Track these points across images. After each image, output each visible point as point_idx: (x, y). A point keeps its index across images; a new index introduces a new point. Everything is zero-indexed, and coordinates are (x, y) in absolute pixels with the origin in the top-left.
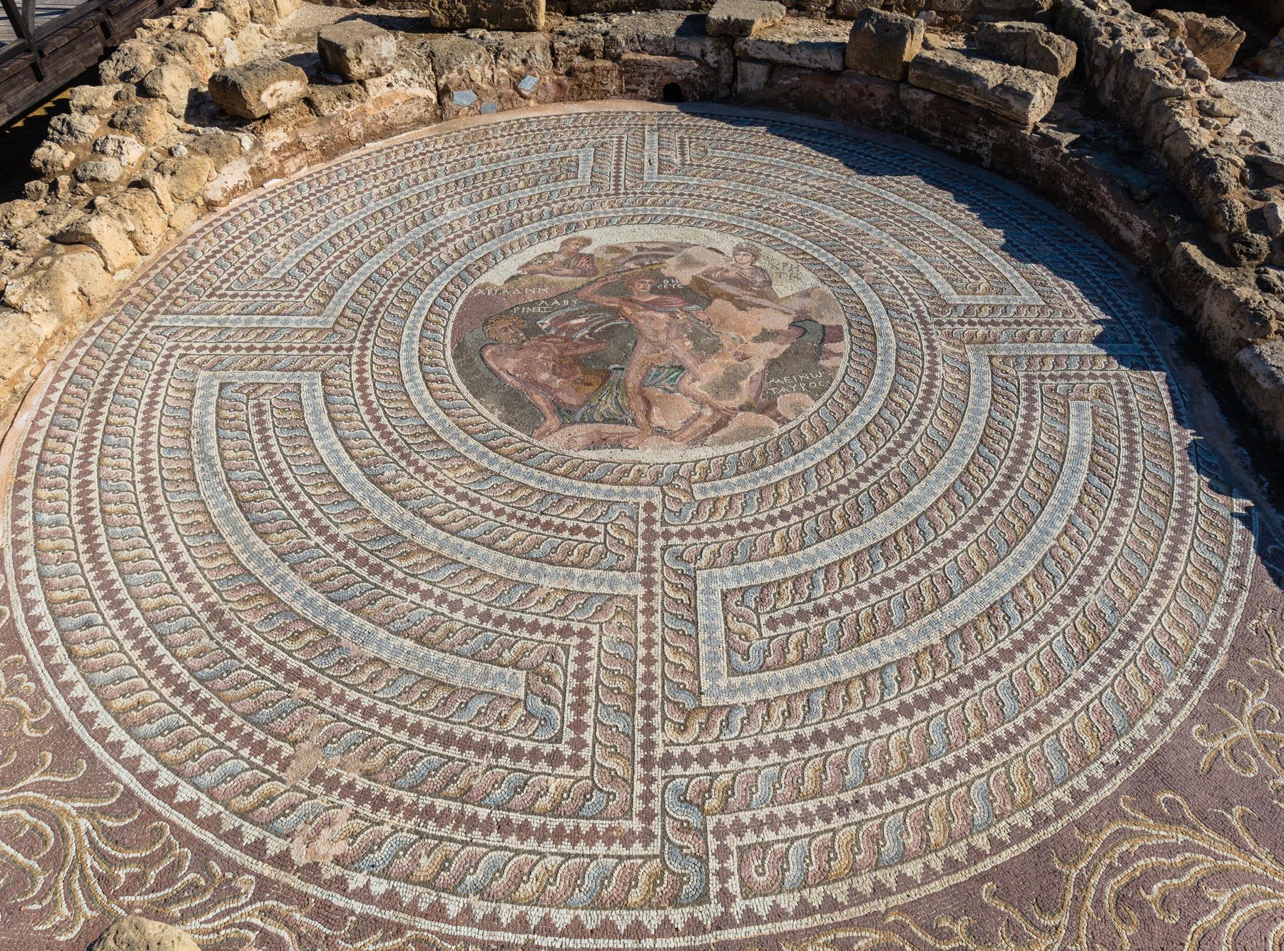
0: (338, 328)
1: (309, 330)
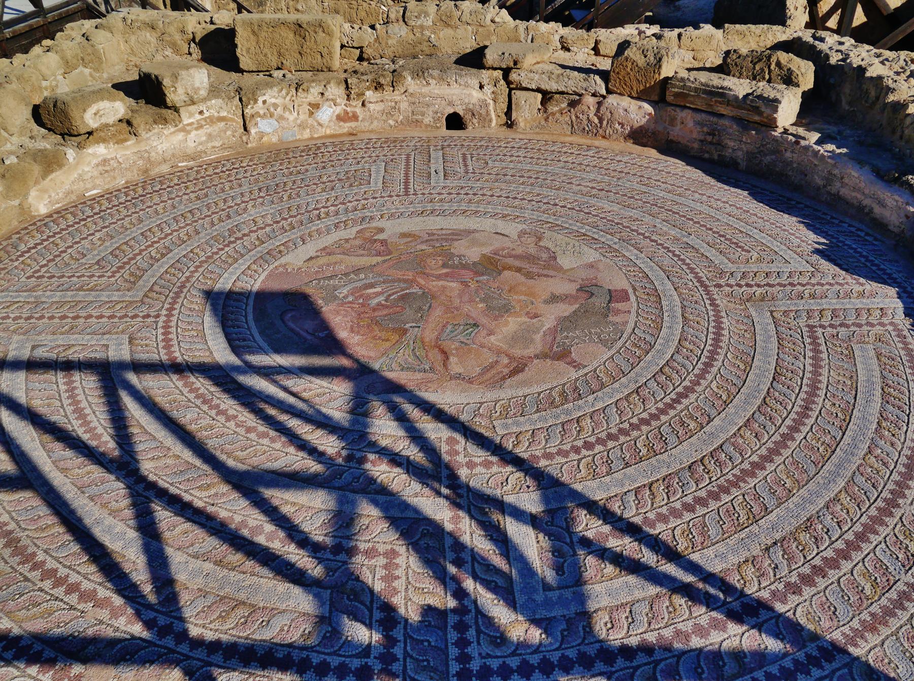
0: (147, 300)
1: (118, 302)
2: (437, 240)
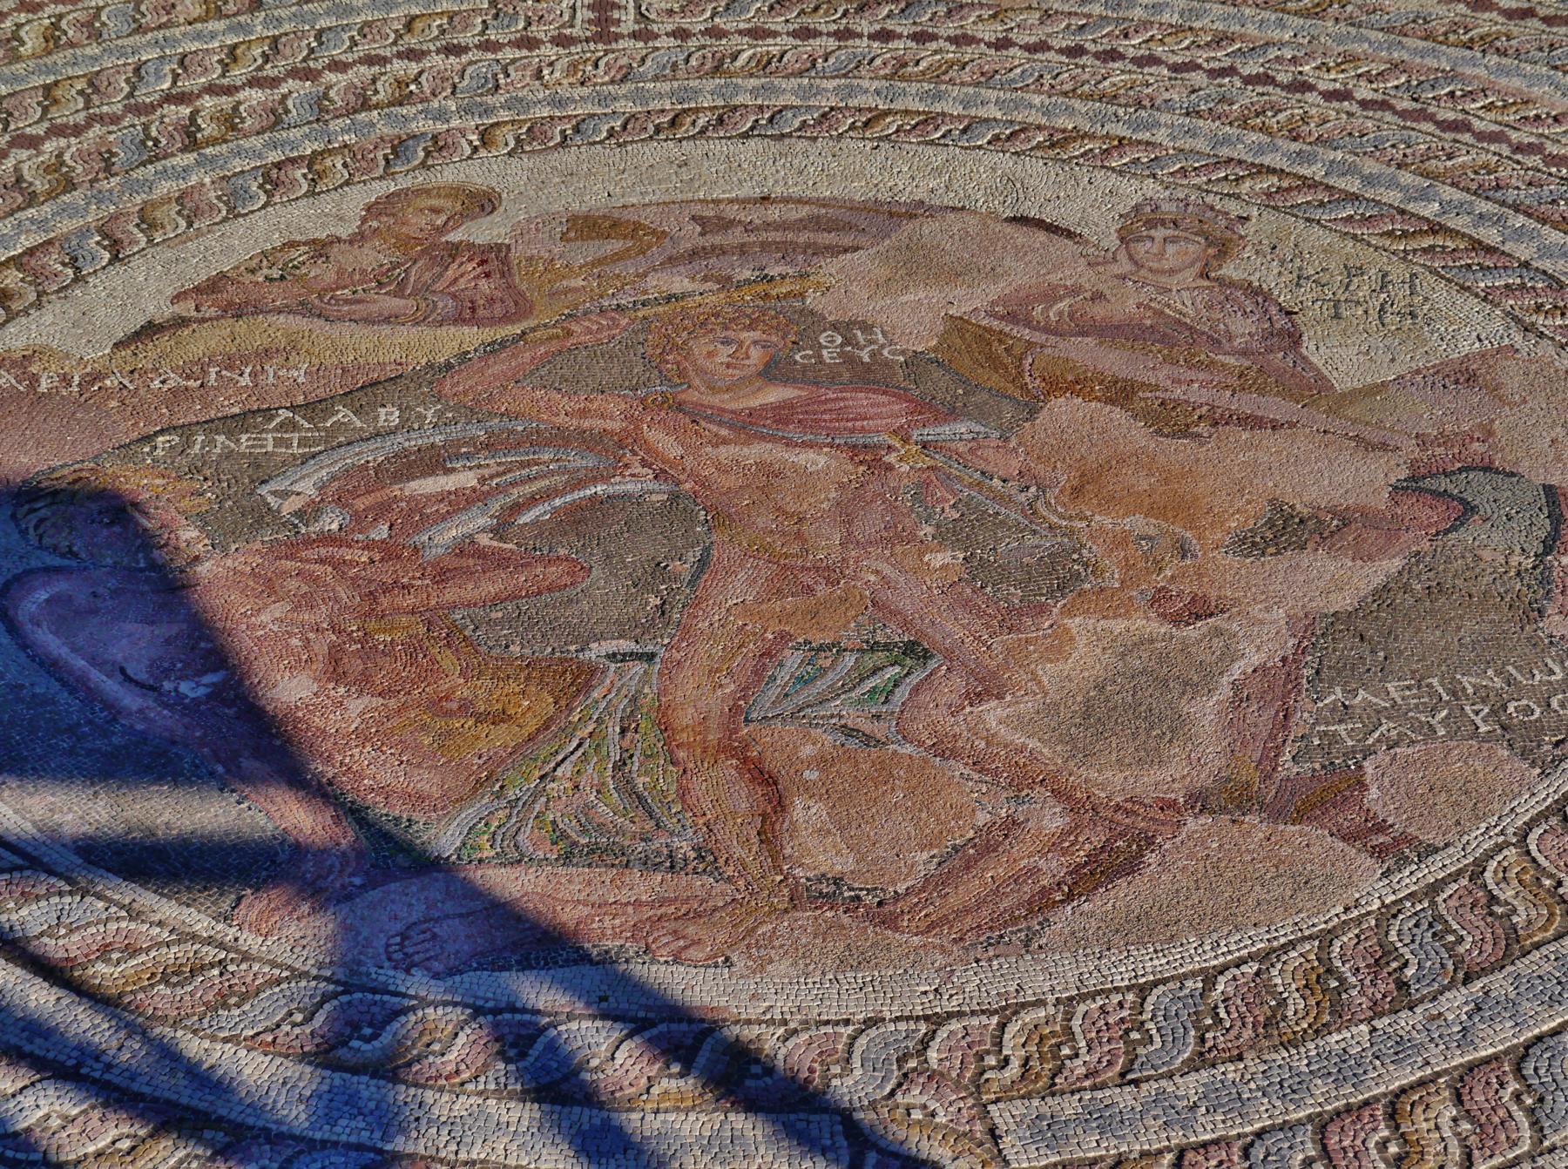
2: (743, 250)
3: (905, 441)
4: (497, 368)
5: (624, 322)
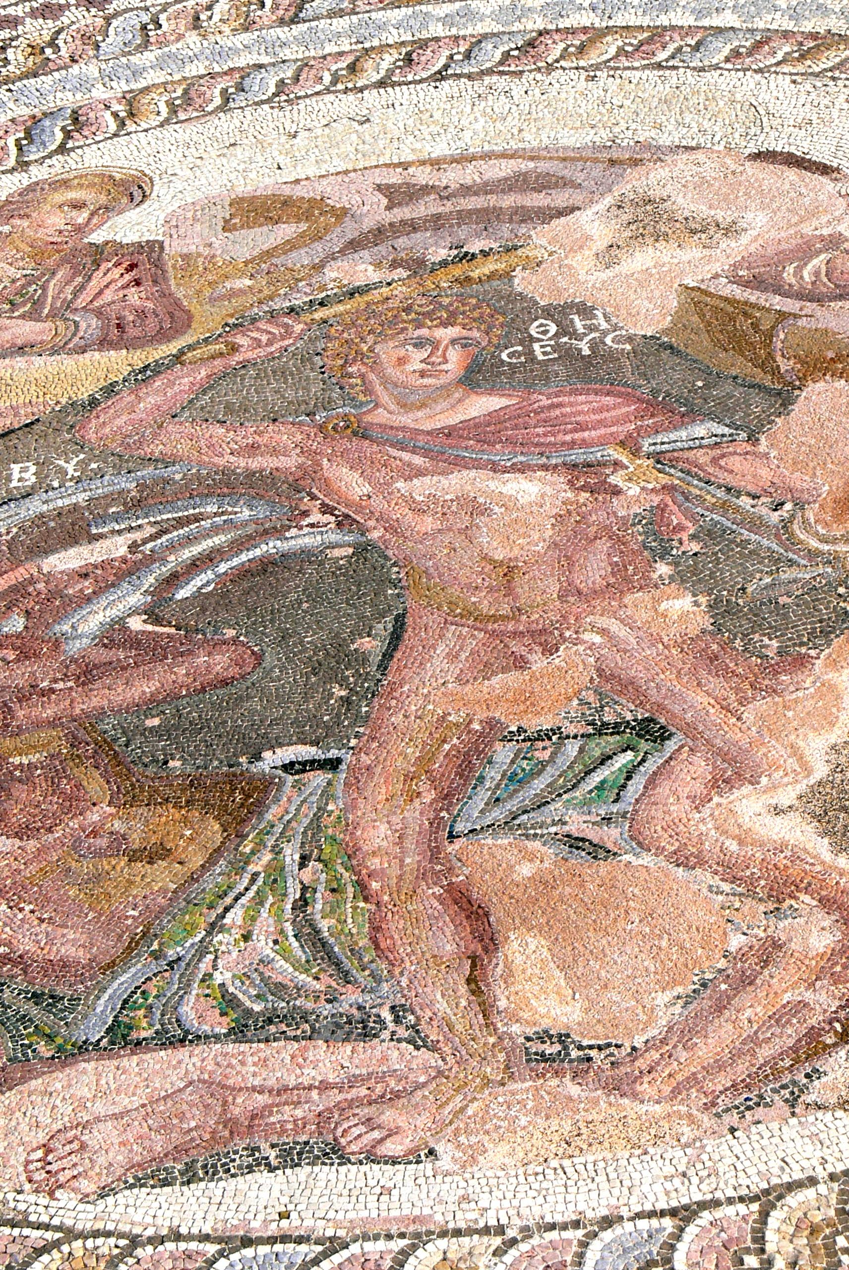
2: (437, 222)
3: (636, 452)
4: (152, 398)
5: (298, 328)
